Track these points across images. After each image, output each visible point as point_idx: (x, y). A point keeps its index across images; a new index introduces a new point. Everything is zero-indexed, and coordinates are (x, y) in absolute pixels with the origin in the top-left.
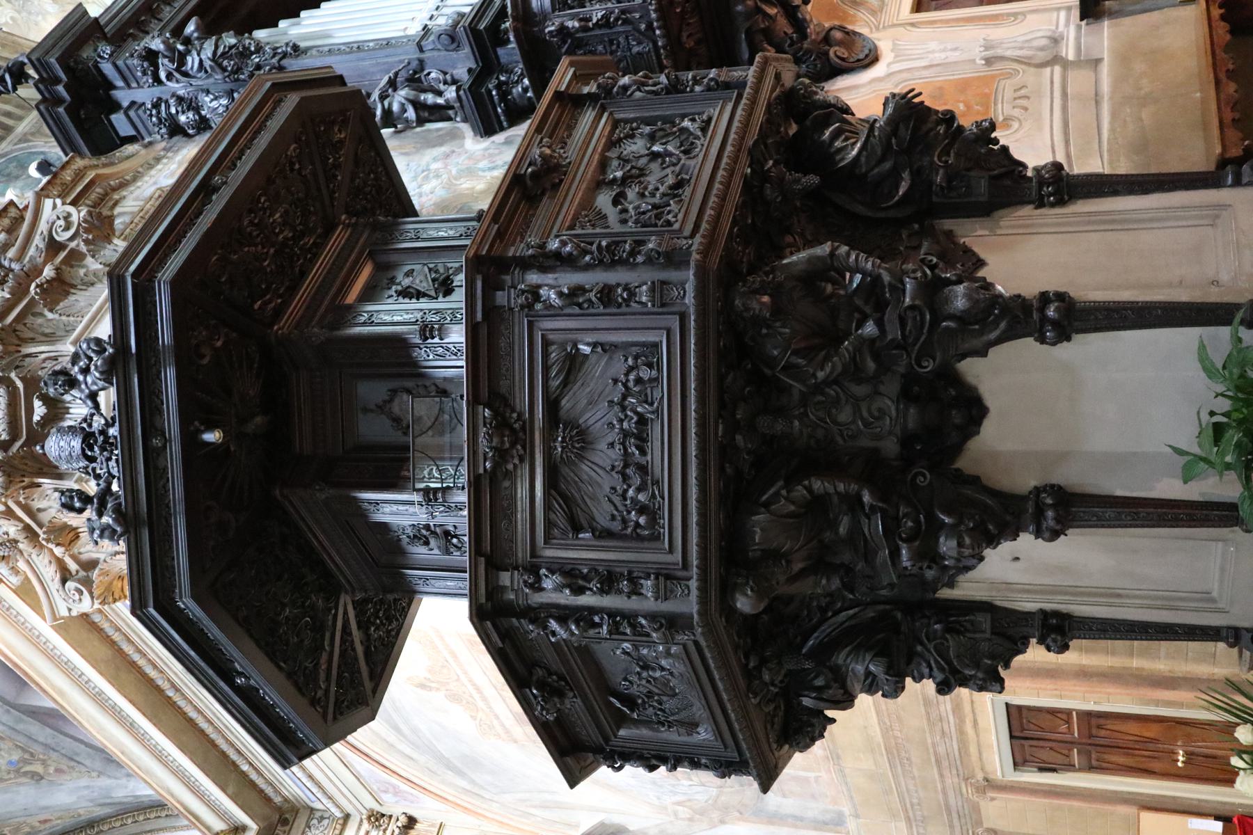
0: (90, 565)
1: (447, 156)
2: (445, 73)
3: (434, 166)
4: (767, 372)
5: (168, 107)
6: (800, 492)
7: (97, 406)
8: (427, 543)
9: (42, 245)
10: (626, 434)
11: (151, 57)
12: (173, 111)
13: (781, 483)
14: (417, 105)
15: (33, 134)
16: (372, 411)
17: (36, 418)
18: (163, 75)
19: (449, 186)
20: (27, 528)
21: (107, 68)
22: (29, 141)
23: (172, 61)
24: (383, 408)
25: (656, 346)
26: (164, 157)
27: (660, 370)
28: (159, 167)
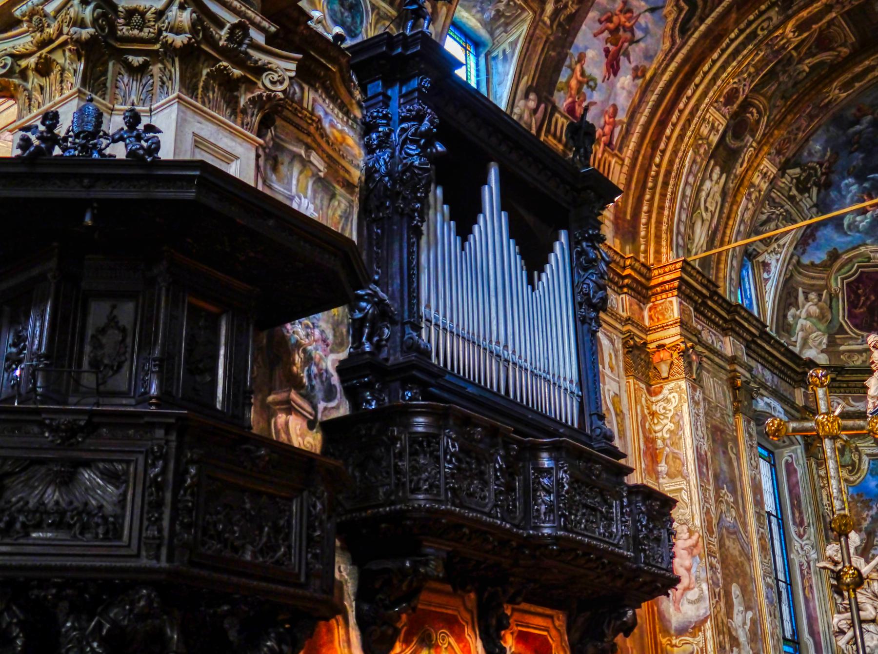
0: (23, 74)
1: (324, 341)
2: (387, 340)
3: (317, 332)
4: (99, 609)
5: (383, 125)
6: (16, 631)
7: (115, 141)
8: (15, 345)
9: (260, 63)
10: (62, 513)
11: (419, 118)
12: (381, 129)
13: (22, 617)
14: (362, 321)
15: (378, 14)
16: (112, 312)
17: (130, 58)
18: (405, 125)
19: (298, 345)
20: (51, 41)
21: (415, 83)
22: (373, 10)
23: (413, 135)
24: (113, 320)
25: (120, 538)
26: (349, 117)
27: (103, 540)
28: (340, 115)
